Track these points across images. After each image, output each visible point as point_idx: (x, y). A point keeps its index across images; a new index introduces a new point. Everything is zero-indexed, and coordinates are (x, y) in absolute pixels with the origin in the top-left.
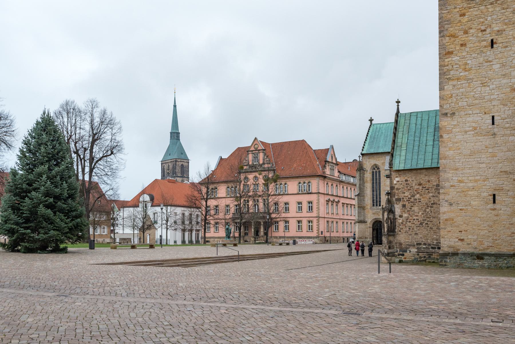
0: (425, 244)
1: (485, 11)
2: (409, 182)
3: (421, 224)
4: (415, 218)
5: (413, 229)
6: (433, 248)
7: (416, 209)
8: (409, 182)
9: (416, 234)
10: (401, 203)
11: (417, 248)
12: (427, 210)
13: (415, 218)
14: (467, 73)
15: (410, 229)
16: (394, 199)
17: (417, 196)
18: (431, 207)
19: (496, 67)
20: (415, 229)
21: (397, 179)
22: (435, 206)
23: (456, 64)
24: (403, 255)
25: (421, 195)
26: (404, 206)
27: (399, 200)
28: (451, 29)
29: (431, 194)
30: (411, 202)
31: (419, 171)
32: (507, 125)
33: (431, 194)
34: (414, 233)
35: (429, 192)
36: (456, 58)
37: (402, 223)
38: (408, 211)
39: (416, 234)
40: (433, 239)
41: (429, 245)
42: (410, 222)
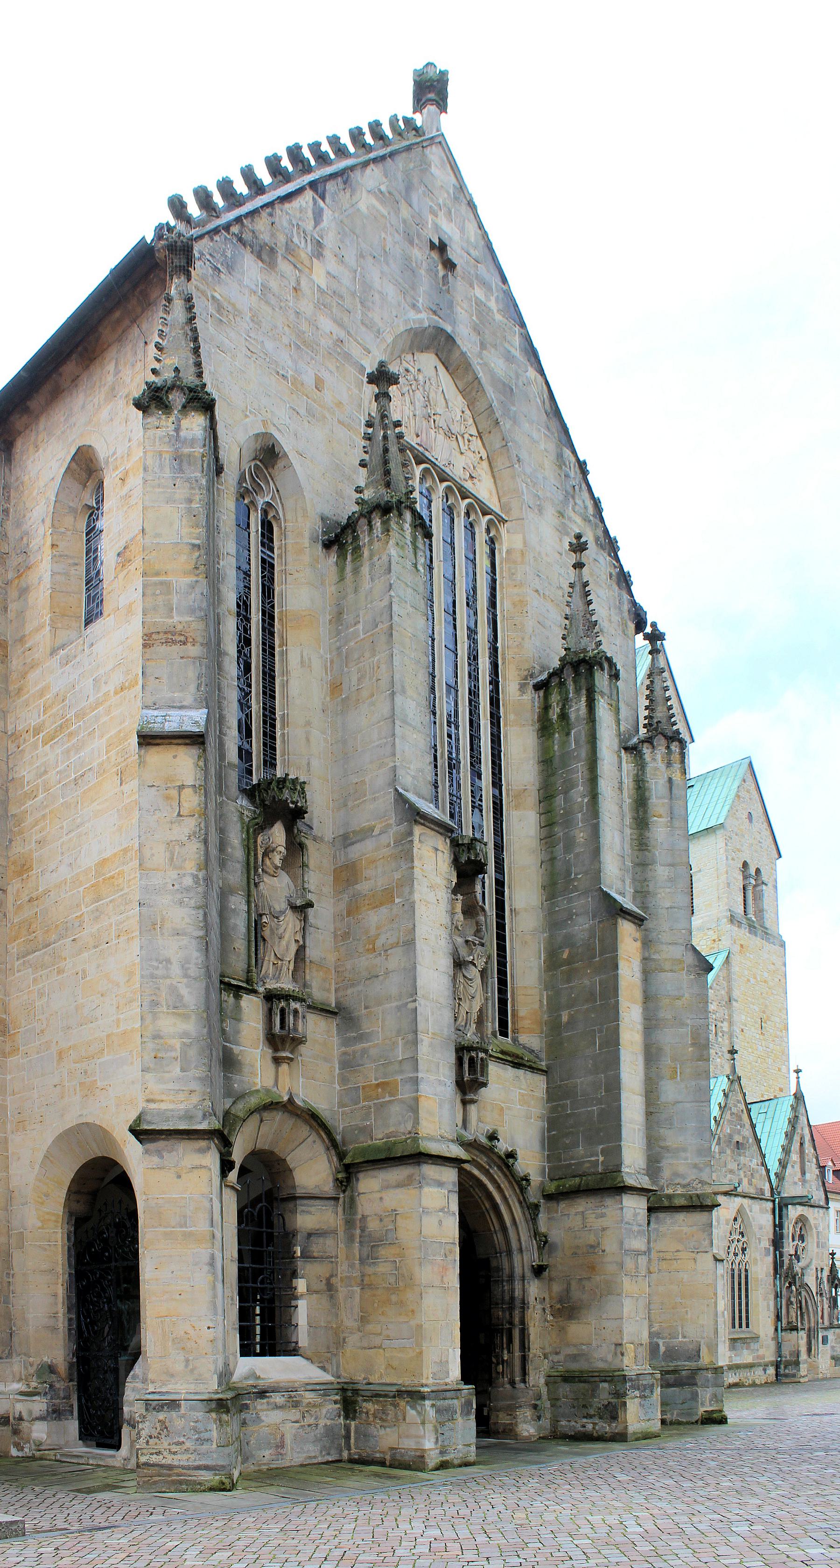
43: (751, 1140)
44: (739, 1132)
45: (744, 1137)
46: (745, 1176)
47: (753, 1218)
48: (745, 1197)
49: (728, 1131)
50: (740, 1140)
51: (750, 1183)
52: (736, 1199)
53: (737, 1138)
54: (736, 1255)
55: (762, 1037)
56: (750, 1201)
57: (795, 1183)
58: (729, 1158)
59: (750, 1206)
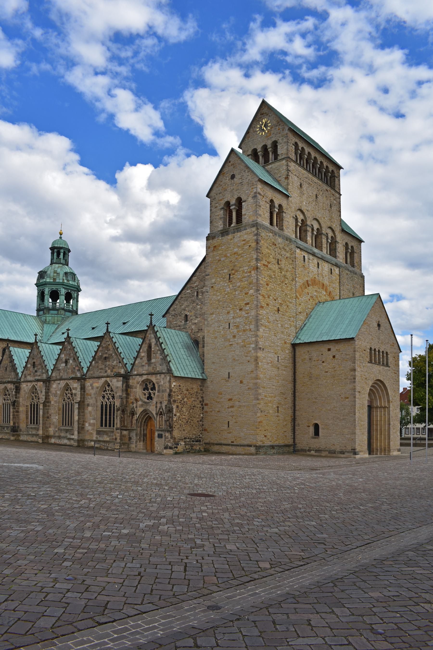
0: (188, 438)
1: (276, 288)
2: (181, 387)
3: (187, 422)
4: (184, 417)
5: (182, 426)
6: (193, 441)
7: (184, 409)
8: (181, 387)
9: (184, 430)
10: (176, 404)
11: (185, 442)
12: (191, 411)
13: (184, 417)
14: (269, 324)
15: (180, 426)
16: (172, 400)
17: (186, 399)
18: (193, 409)
19: (280, 325)
20: (184, 426)
21: (174, 384)
22: (195, 408)
23: (265, 316)
24: (177, 448)
25: (188, 399)
26: (177, 407)
27: (174, 401)
28: (263, 291)
29: (193, 399)
30: (182, 404)
31: (187, 379)
32: (283, 364)
33: (193, 399)
34: (183, 429)
35: (192, 397)
36: (264, 312)
37: (176, 421)
38: (180, 411)
39: (184, 430)
40: (193, 434)
41: (191, 439)
42: (181, 420)
43: (113, 354)
44: (106, 353)
45: (109, 354)
46: (109, 369)
47: (113, 385)
48: (107, 377)
49: (100, 354)
50: (107, 355)
51: (112, 371)
52: (103, 379)
53: (105, 356)
54: (108, 399)
55: (229, 283)
56: (111, 378)
57: (143, 366)
58: (100, 364)
59: (110, 380)
